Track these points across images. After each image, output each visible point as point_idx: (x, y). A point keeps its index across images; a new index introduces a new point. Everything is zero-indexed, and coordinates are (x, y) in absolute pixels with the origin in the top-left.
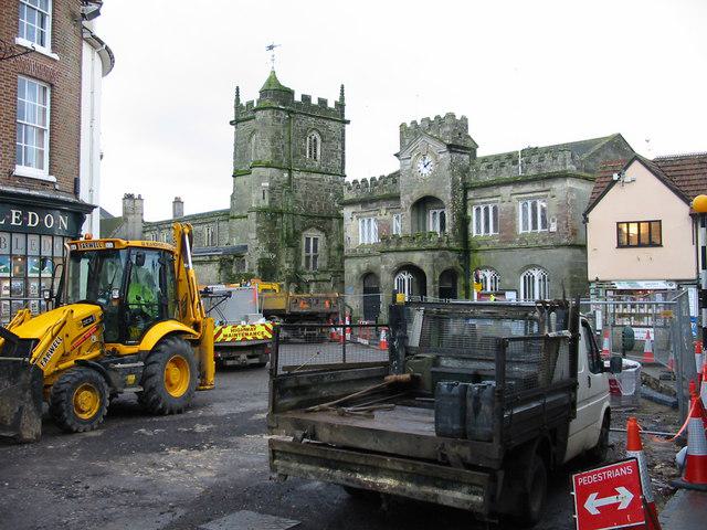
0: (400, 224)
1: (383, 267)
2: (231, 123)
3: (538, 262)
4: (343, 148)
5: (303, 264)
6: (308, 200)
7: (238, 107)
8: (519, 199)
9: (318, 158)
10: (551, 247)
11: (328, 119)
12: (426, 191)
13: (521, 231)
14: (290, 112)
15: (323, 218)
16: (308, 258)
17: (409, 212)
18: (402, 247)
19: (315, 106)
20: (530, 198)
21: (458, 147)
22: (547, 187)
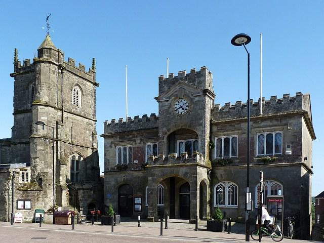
4: (95, 102)
9: (80, 106)
11: (86, 79)
15: (83, 147)
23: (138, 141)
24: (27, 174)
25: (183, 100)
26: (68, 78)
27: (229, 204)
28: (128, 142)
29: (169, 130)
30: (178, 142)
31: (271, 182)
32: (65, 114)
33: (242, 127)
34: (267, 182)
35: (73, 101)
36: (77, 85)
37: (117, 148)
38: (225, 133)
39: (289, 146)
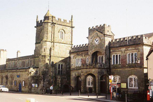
0: (88, 59)
1: (82, 74)
2: (35, 27)
5: (57, 73)
7: (37, 22)
11: (67, 26)
12: (97, 50)
16: (59, 71)
23: (83, 56)
25: (97, 38)
28: (80, 56)
30: (99, 56)
36: (62, 29)
37: (76, 59)
39: (139, 60)
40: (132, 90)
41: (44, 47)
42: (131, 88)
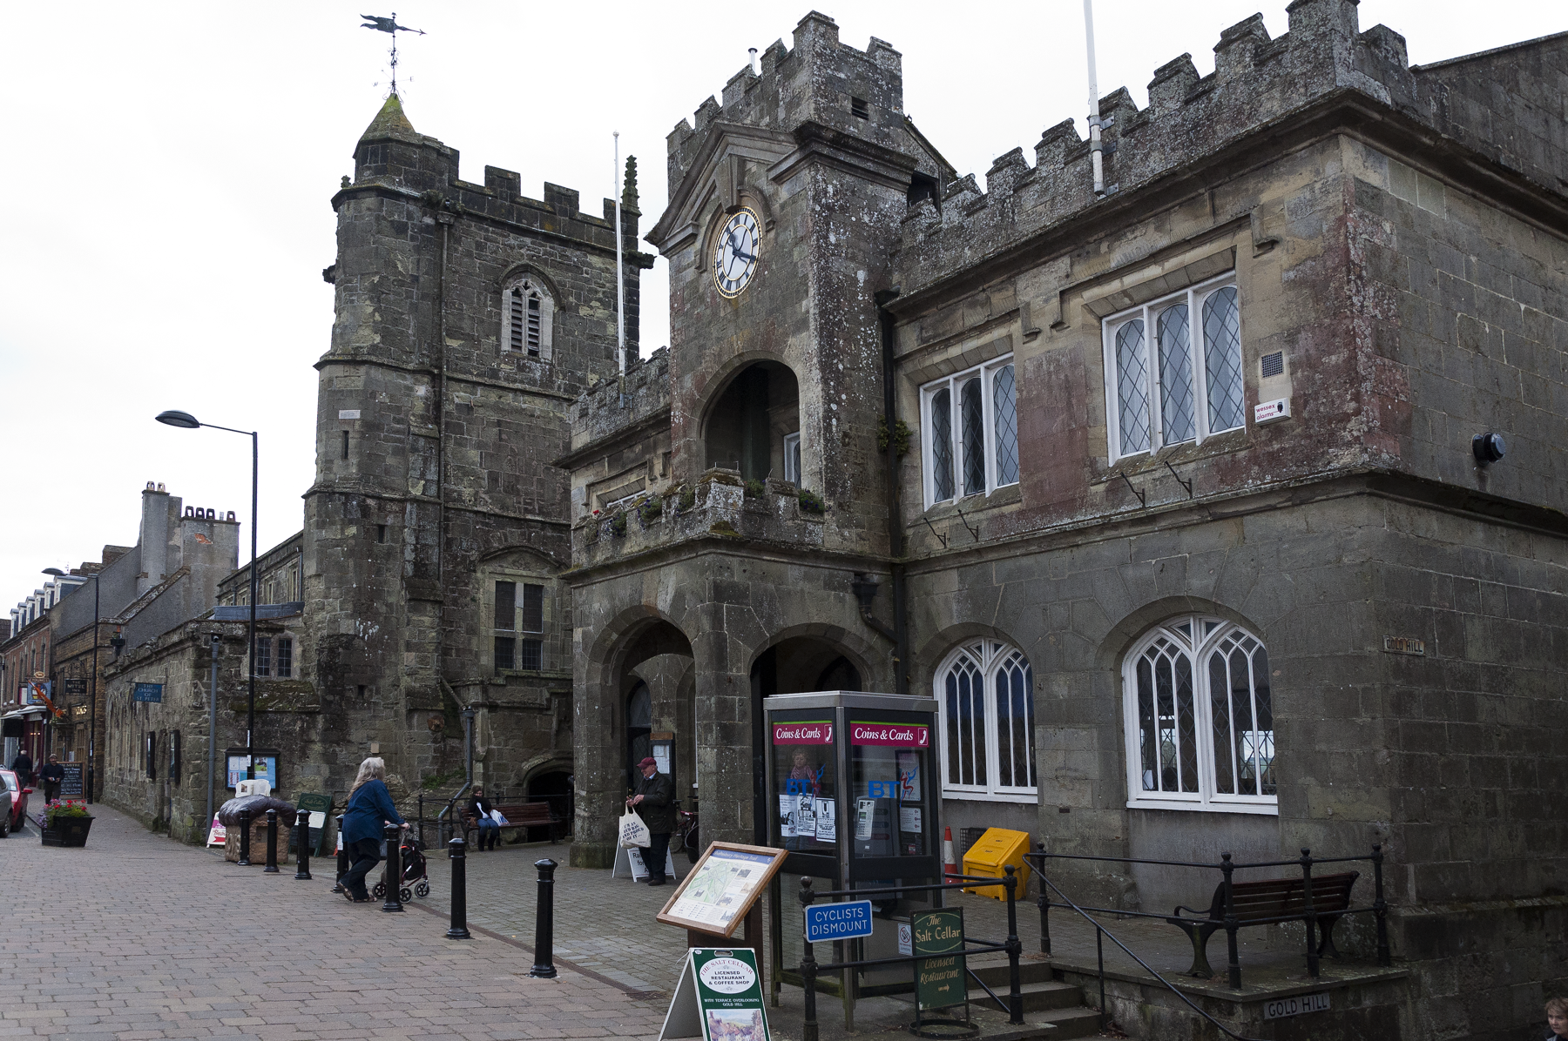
3: (1198, 583)
6: (505, 469)
8: (1099, 313)
9: (546, 354)
10: (1266, 503)
11: (579, 246)
12: (736, 343)
13: (1114, 455)
14: (430, 205)
17: (696, 438)
18: (631, 547)
19: (529, 203)
20: (1149, 292)
21: (841, 141)
22: (1231, 209)
23: (658, 468)
24: (286, 645)
26: (479, 246)
27: (1005, 780)
29: (699, 383)
31: (1210, 627)
32: (459, 395)
33: (1023, 298)
34: (1186, 629)
35: (506, 331)
36: (525, 269)
38: (955, 351)
39: (1272, 367)
40: (1184, 842)
41: (343, 414)
42: (1178, 800)
